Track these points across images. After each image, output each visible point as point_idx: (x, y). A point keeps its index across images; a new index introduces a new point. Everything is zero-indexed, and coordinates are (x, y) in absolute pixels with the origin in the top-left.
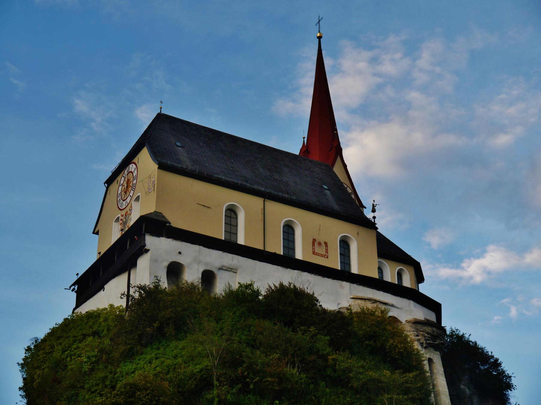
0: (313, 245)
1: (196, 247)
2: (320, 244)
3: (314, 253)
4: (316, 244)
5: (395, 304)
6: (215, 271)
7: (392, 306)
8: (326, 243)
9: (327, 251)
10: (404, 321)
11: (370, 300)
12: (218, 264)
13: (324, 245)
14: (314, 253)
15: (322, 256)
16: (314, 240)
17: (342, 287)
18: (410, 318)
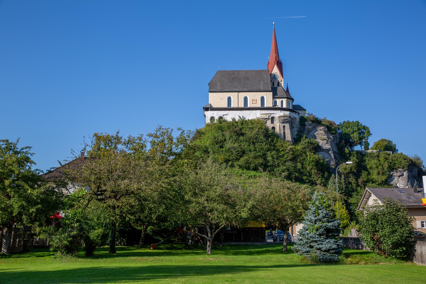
0: (252, 101)
1: (217, 111)
2: (254, 100)
3: (252, 103)
4: (253, 100)
5: (274, 113)
6: (222, 116)
7: (273, 114)
8: (256, 100)
9: (256, 102)
10: (276, 117)
11: (265, 114)
12: (223, 114)
13: (255, 100)
14: (252, 103)
15: (255, 103)
16: (253, 100)
17: (258, 112)
18: (278, 116)
